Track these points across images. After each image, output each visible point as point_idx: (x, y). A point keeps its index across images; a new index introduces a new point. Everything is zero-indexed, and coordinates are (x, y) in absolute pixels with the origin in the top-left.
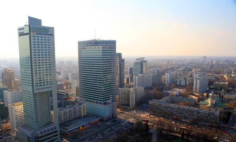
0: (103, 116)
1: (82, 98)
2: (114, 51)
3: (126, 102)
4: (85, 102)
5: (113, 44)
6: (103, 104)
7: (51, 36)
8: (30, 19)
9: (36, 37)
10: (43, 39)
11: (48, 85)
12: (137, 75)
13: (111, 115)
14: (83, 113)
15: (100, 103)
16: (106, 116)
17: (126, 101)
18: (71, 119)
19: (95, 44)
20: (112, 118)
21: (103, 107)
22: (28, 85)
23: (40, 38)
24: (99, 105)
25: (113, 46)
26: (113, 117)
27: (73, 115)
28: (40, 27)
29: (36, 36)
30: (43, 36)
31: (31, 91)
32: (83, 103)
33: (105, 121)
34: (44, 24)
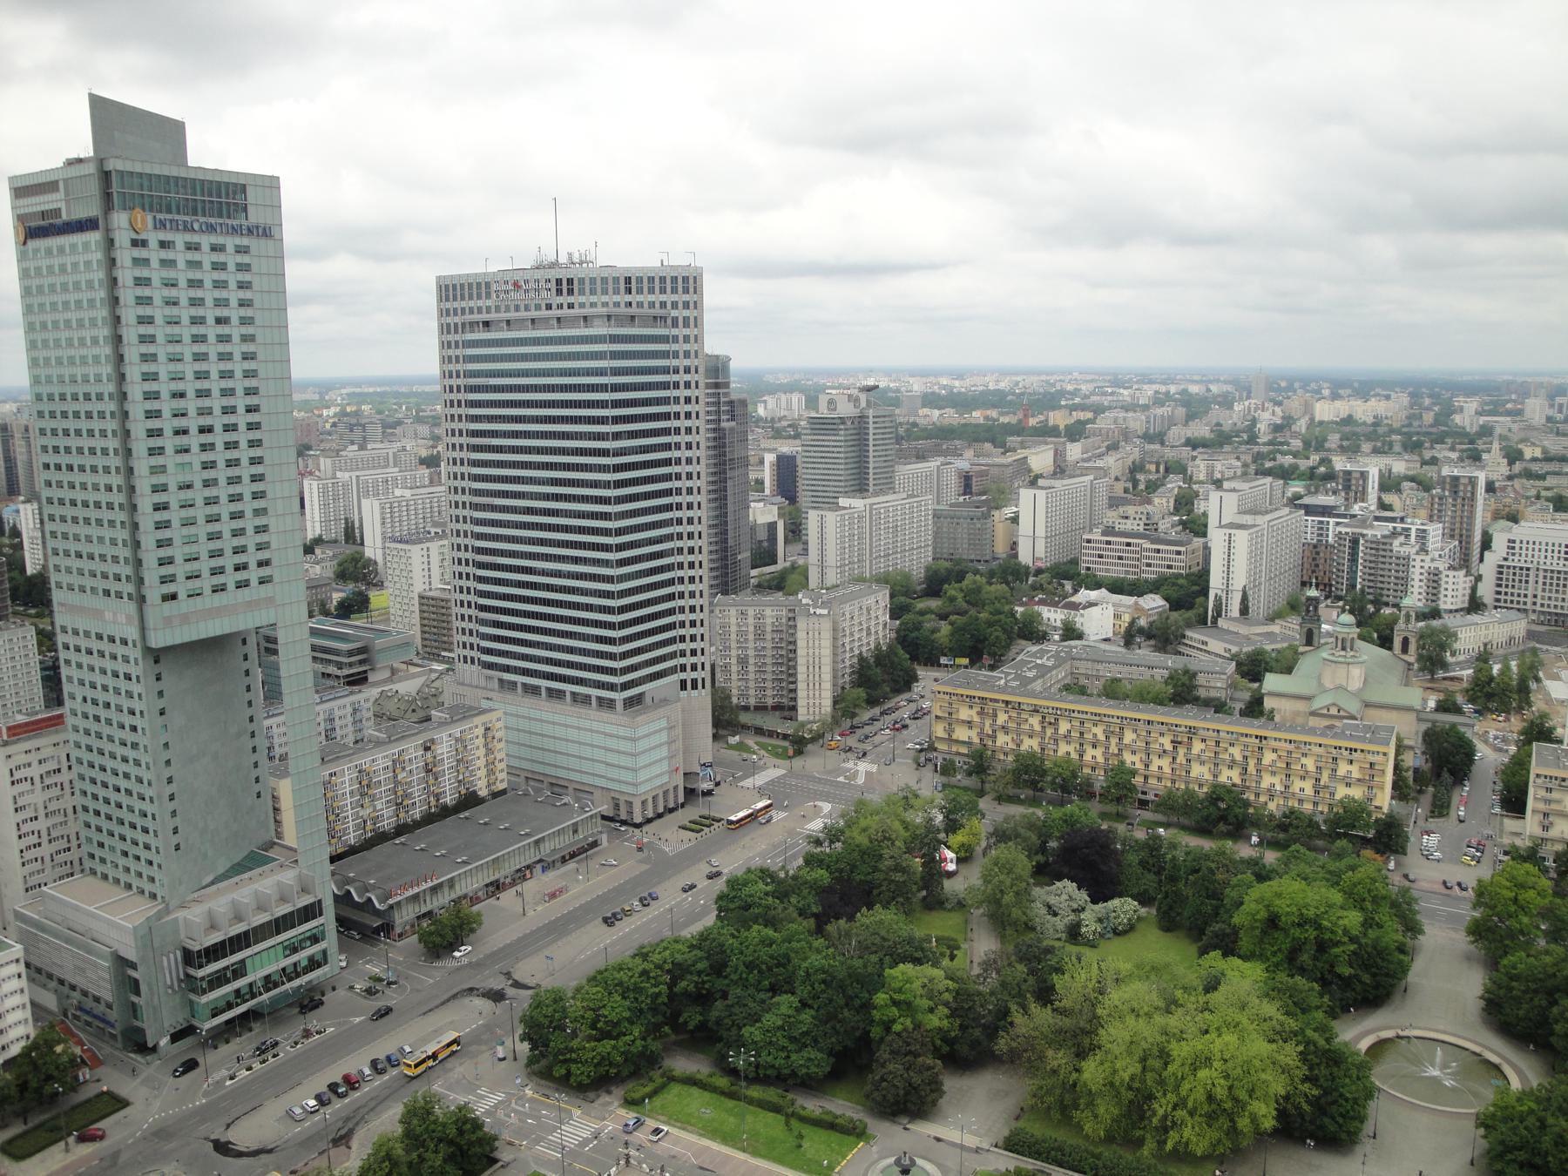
0: (624, 788)
1: (476, 668)
2: (686, 339)
5: (686, 291)
6: (619, 706)
7: (263, 241)
8: (106, 114)
9: (153, 244)
10: (207, 258)
13: (679, 781)
14: (482, 773)
16: (642, 789)
19: (559, 292)
20: (681, 800)
21: (622, 732)
22: (107, 593)
23: (181, 257)
25: (686, 305)
26: (690, 793)
28: (174, 172)
29: (153, 238)
30: (206, 241)
31: (132, 633)
32: (485, 704)
33: (638, 826)
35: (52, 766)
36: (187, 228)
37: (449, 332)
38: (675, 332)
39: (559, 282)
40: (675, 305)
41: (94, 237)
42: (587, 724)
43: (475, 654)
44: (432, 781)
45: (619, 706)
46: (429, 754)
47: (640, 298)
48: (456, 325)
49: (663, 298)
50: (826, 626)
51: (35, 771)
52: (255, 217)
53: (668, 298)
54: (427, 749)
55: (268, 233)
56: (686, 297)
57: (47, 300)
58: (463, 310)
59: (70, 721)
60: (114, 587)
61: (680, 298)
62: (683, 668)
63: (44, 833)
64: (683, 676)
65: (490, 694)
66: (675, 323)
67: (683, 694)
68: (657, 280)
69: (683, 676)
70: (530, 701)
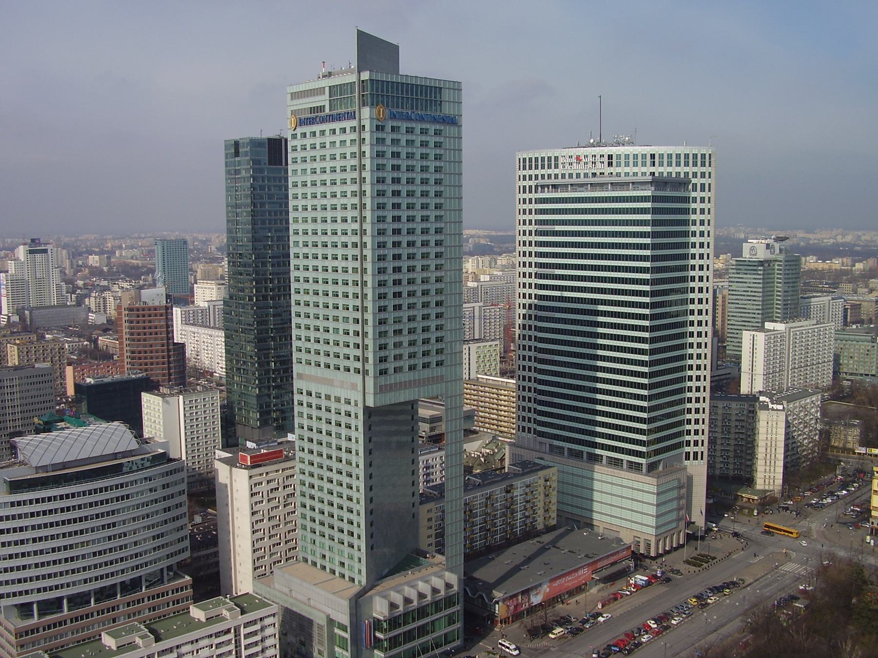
1: (531, 436)
3: (731, 467)
4: (545, 456)
9: (388, 129)
11: (426, 366)
12: (762, 329)
14: (541, 512)
17: (731, 460)
18: (489, 539)
19: (610, 164)
23: (418, 139)
27: (499, 522)
30: (418, 126)
35: (273, 485)
36: (409, 119)
38: (693, 194)
39: (610, 157)
40: (695, 175)
41: (348, 124)
42: (615, 480)
43: (532, 425)
44: (509, 516)
46: (509, 495)
47: (619, 170)
48: (530, 187)
49: (687, 169)
50: (782, 417)
51: (264, 488)
52: (447, 110)
53: (690, 169)
54: (508, 492)
55: (453, 121)
56: (703, 169)
58: (536, 177)
59: (299, 454)
60: (343, 363)
61: (699, 169)
62: (688, 443)
63: (267, 531)
64: (687, 449)
65: (542, 455)
66: (695, 189)
67: (686, 463)
68: (631, 157)
69: (687, 449)
70: (573, 462)
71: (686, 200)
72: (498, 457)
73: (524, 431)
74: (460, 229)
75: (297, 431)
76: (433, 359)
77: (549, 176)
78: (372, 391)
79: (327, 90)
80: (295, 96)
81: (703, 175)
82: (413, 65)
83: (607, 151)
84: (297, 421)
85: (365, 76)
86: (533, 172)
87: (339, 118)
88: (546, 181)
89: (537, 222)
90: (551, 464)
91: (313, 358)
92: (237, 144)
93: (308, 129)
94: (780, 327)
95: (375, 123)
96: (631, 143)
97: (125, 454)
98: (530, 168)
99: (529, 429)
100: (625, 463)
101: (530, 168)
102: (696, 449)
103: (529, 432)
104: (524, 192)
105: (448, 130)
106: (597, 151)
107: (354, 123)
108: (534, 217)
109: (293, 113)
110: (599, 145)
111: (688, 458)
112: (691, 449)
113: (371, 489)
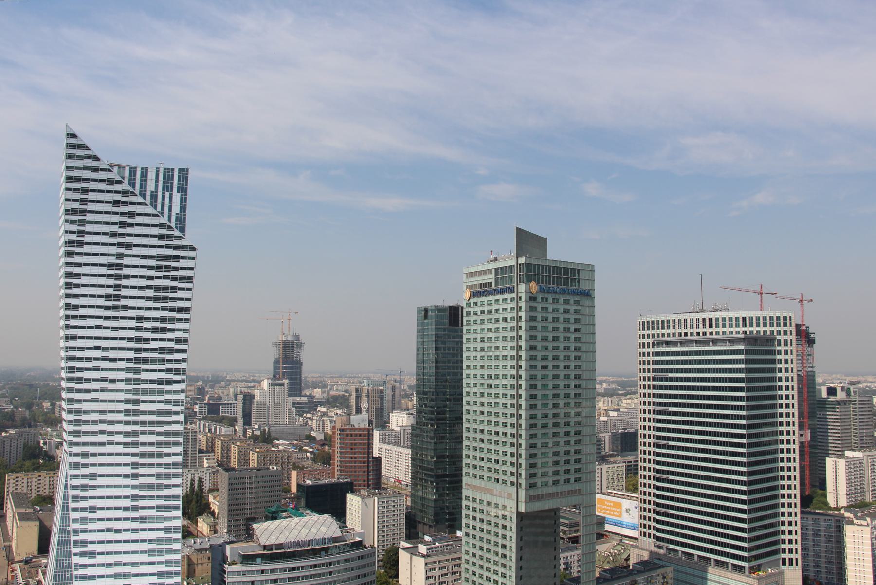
1: (652, 540)
5: (785, 325)
6: (747, 570)
11: (567, 481)
12: (842, 456)
15: (740, 569)
24: (729, 575)
34: (556, 253)
35: (444, 571)
36: (555, 292)
37: (644, 347)
38: (778, 348)
39: (710, 320)
40: (779, 333)
41: (508, 296)
43: (653, 532)
45: (747, 570)
47: (718, 330)
48: (648, 343)
49: (772, 329)
52: (584, 286)
53: (775, 329)
55: (588, 294)
56: (785, 328)
57: (479, 327)
58: (653, 335)
60: (502, 477)
61: (782, 329)
62: (784, 551)
64: (783, 556)
66: (779, 344)
67: (783, 567)
69: (783, 556)
71: (773, 352)
72: (624, 556)
73: (645, 535)
74: (594, 375)
75: (464, 529)
76: (572, 477)
77: (663, 335)
78: (523, 500)
79: (493, 271)
80: (470, 275)
81: (785, 333)
82: (558, 253)
83: (707, 316)
84: (464, 521)
85: (522, 260)
86: (650, 332)
87: (502, 291)
88: (661, 339)
89: (655, 370)
90: (668, 564)
91: (478, 472)
92: (426, 310)
93: (478, 300)
94: (858, 455)
95: (529, 295)
96: (727, 309)
97: (335, 540)
98: (648, 329)
99: (650, 534)
100: (730, 565)
101: (648, 329)
102: (791, 556)
103: (650, 537)
104: (644, 347)
105: (585, 301)
106: (701, 316)
107: (514, 295)
108: (651, 367)
109: (468, 287)
110: (702, 311)
111: (784, 563)
112: (787, 556)
113: (521, 579)
